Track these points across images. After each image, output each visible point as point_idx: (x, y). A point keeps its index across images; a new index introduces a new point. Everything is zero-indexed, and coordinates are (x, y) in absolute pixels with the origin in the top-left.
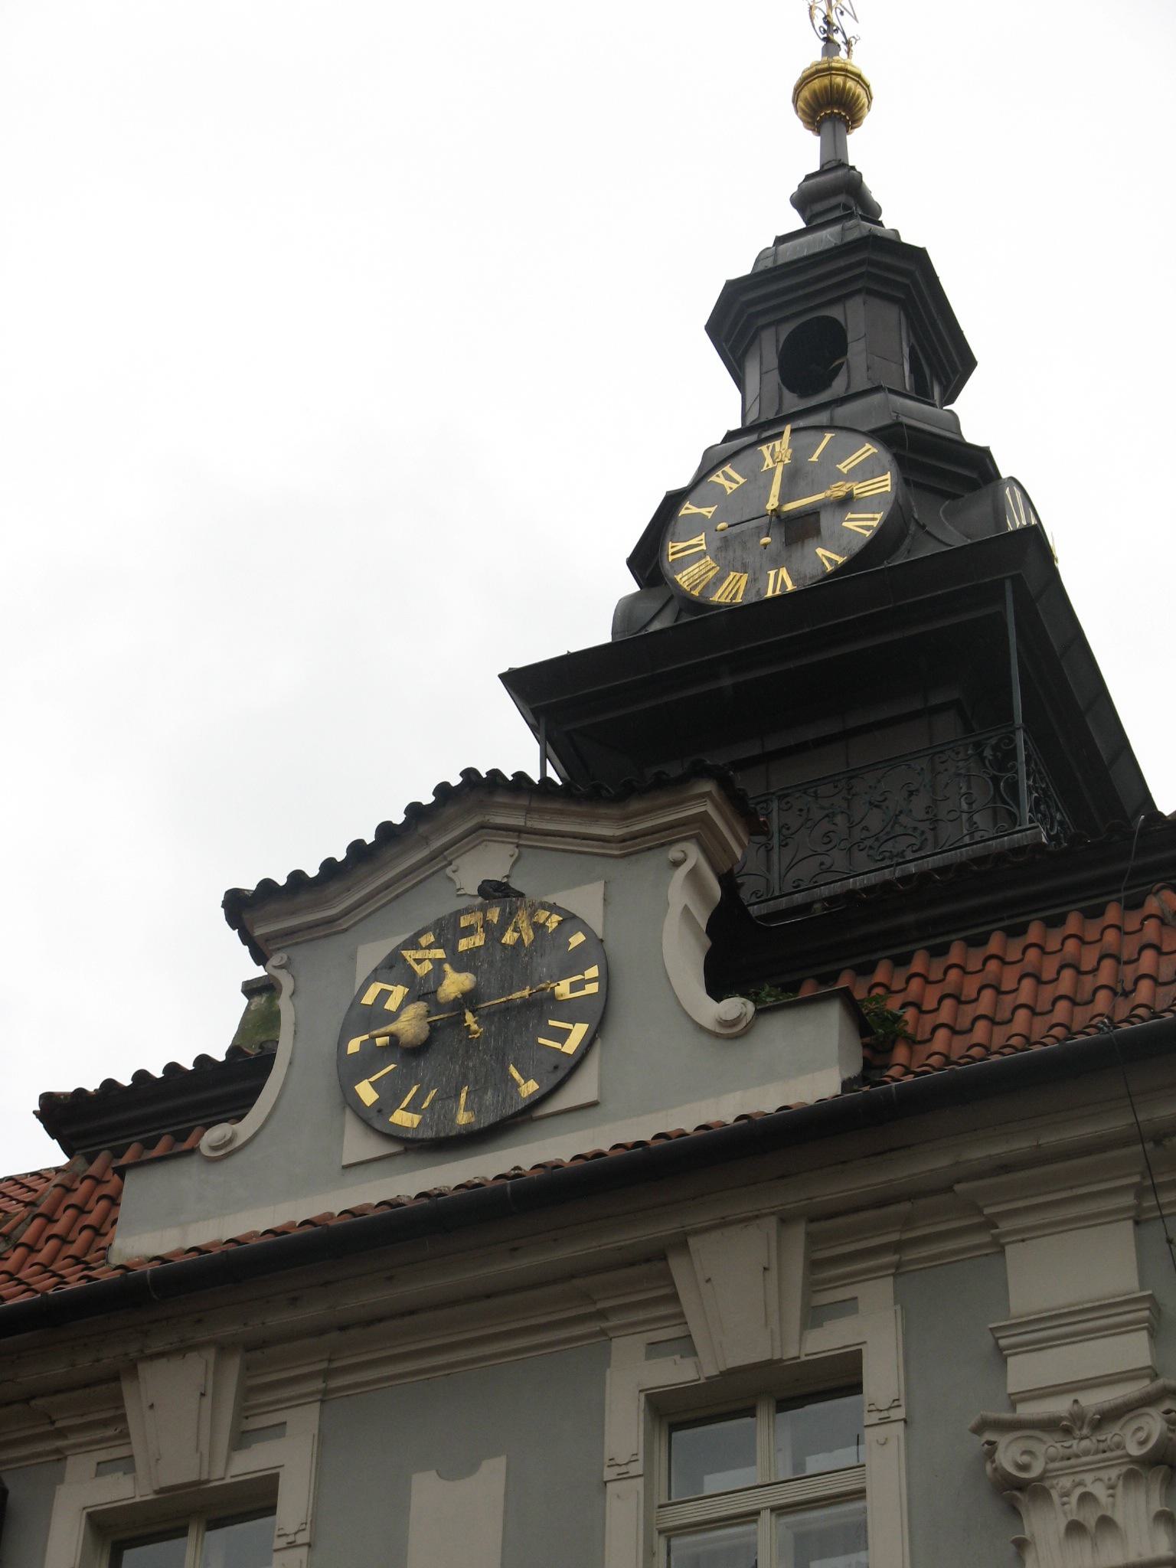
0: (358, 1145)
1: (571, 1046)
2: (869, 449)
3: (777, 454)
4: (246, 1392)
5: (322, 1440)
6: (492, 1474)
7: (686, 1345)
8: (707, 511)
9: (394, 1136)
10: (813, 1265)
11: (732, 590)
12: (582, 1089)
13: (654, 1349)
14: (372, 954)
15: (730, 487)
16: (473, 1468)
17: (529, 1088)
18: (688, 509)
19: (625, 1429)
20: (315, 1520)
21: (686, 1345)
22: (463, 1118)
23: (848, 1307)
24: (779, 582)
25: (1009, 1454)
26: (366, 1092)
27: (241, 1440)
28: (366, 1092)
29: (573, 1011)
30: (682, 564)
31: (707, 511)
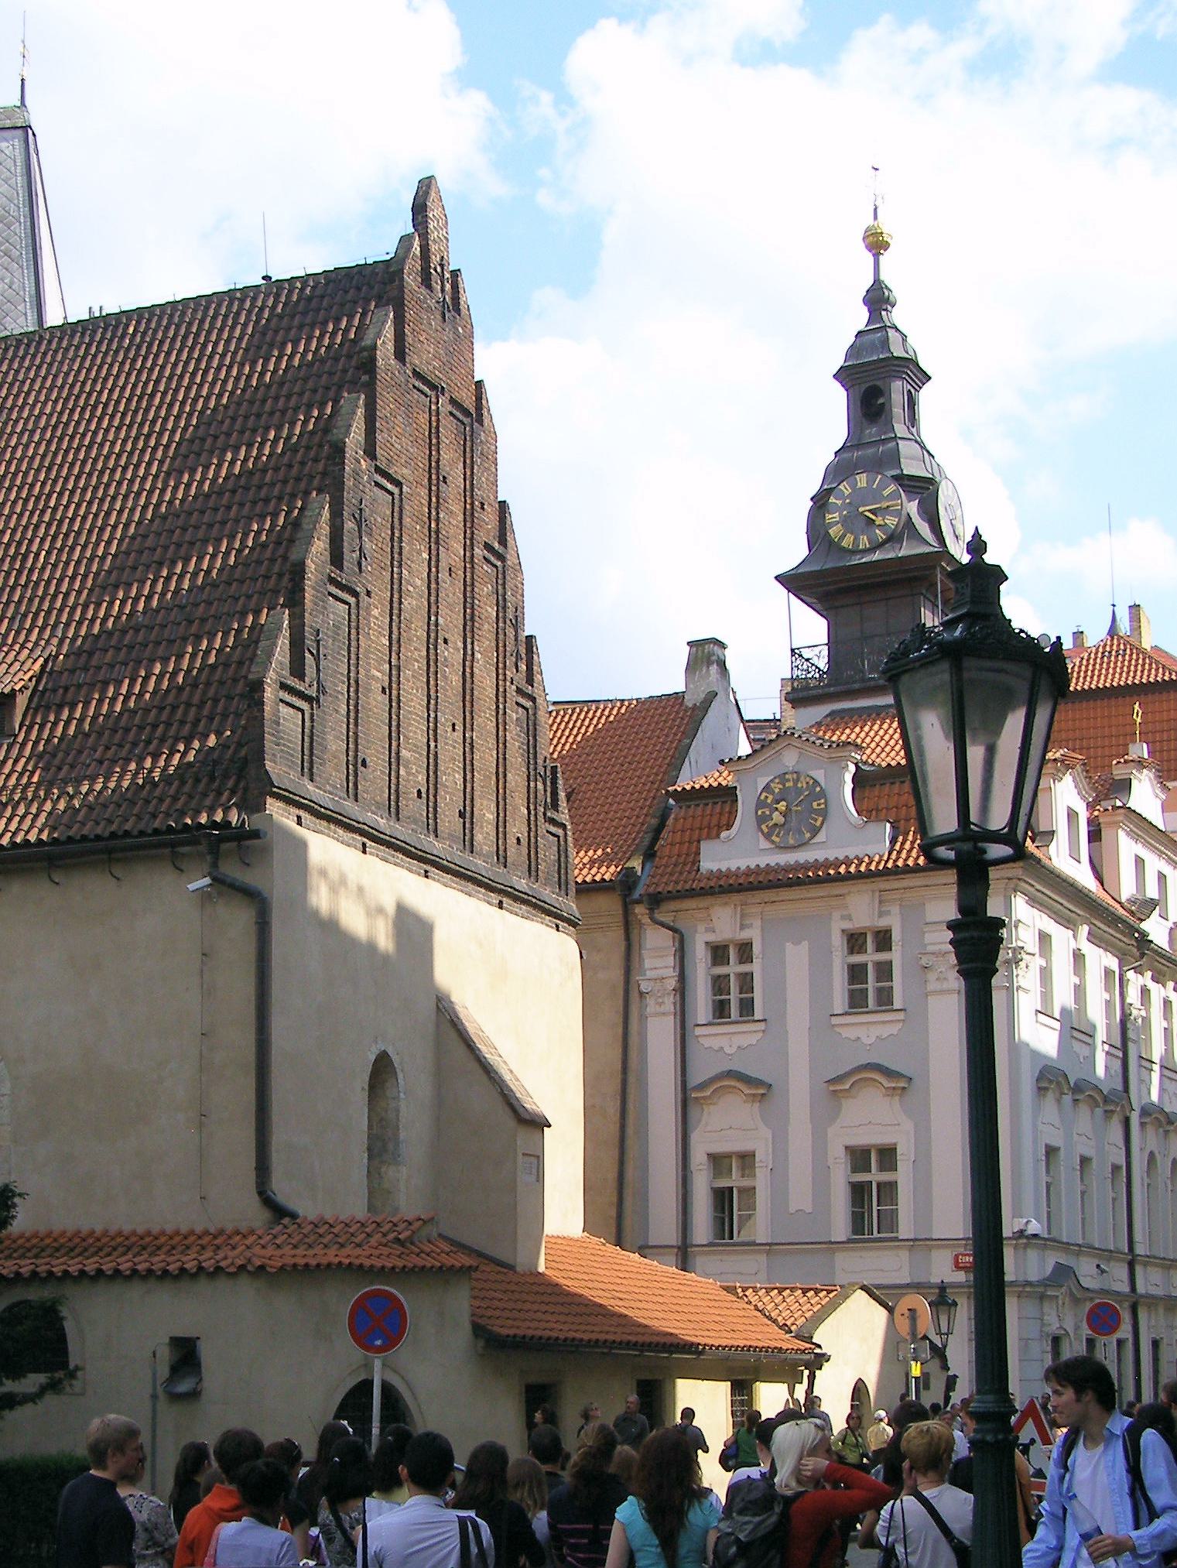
0: (764, 844)
1: (818, 824)
2: (892, 487)
3: (862, 480)
4: (742, 916)
5: (762, 929)
6: (805, 944)
7: (849, 918)
8: (839, 502)
9: (773, 842)
10: (880, 902)
11: (847, 542)
12: (821, 837)
13: (843, 918)
14: (762, 783)
15: (847, 493)
16: (799, 943)
17: (808, 835)
18: (832, 500)
19: (838, 942)
20: (763, 952)
21: (849, 918)
22: (791, 842)
23: (888, 913)
24: (864, 542)
25: (923, 962)
26: (766, 830)
27: (742, 927)
28: (764, 827)
29: (818, 812)
30: (831, 525)
31: (839, 502)
